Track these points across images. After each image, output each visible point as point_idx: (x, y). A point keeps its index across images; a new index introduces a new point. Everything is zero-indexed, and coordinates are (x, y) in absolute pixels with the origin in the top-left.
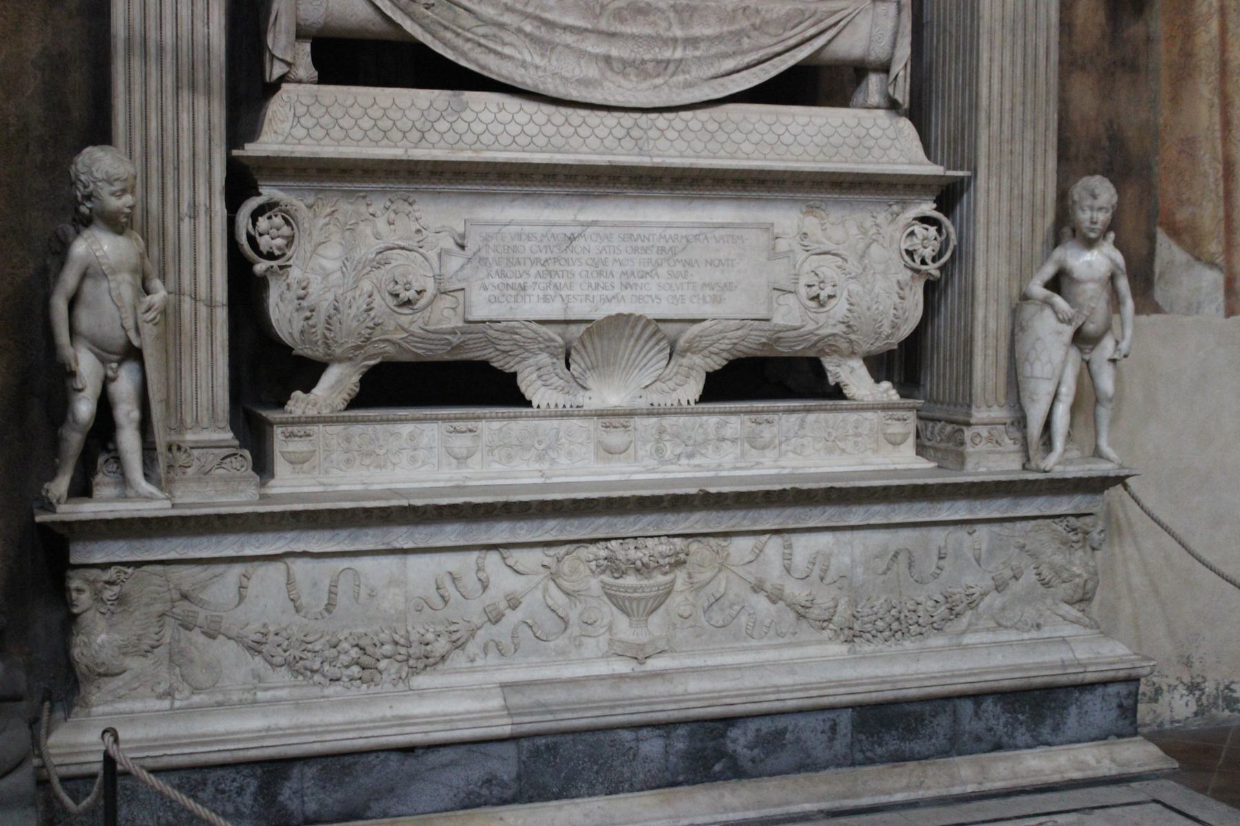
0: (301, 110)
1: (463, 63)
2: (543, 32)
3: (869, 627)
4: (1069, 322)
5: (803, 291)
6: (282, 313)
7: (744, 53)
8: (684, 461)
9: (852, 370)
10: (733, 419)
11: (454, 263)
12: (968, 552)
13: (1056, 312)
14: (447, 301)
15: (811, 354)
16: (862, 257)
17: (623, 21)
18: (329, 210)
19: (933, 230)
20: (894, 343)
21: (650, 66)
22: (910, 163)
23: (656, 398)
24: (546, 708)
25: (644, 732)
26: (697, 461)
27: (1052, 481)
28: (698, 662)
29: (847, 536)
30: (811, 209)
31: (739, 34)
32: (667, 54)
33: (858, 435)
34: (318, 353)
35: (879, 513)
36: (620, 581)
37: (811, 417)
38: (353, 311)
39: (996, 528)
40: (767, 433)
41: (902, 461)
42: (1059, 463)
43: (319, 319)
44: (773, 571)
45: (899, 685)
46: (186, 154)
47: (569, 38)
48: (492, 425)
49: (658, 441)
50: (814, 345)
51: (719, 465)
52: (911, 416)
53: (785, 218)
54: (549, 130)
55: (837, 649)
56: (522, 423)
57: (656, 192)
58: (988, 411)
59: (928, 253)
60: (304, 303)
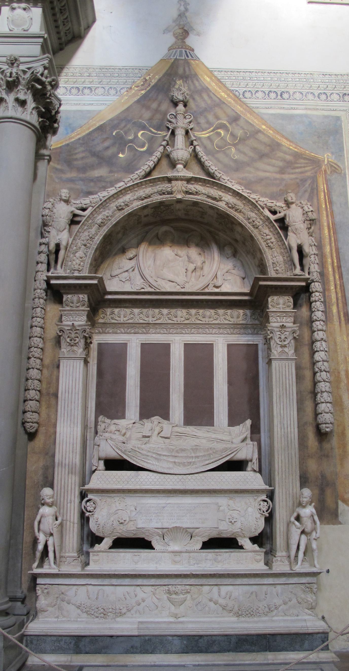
0: (99, 477)
1: (138, 465)
2: (158, 457)
3: (244, 613)
4: (299, 528)
5: (227, 520)
6: (93, 526)
7: (211, 459)
8: (196, 565)
9: (245, 541)
10: (210, 554)
11: (134, 513)
12: (275, 593)
13: (295, 526)
14: (132, 523)
15: (233, 537)
16: (245, 511)
17: (178, 453)
18: (104, 501)
19: (266, 503)
20: (257, 534)
21: (186, 463)
22: (260, 485)
23: (188, 548)
24: (148, 628)
25: (175, 638)
26: (199, 565)
27: (296, 573)
28: (193, 620)
29: (237, 587)
30: (231, 499)
31: (209, 455)
32: (191, 460)
33: (246, 559)
34: (101, 535)
35: (245, 581)
36: (171, 596)
37: (233, 554)
38: (108, 525)
39: (283, 586)
40: (219, 558)
41: (260, 567)
42: (299, 568)
43: (101, 527)
44: (215, 596)
45: (248, 630)
46: (70, 488)
47: (165, 458)
48: (144, 553)
49: (189, 559)
50: (233, 534)
51: (205, 567)
52: (263, 554)
53: (223, 501)
54: (160, 480)
55: (235, 619)
56: (152, 554)
57: (187, 495)
58: (280, 553)
59: (265, 509)
60: (97, 523)
